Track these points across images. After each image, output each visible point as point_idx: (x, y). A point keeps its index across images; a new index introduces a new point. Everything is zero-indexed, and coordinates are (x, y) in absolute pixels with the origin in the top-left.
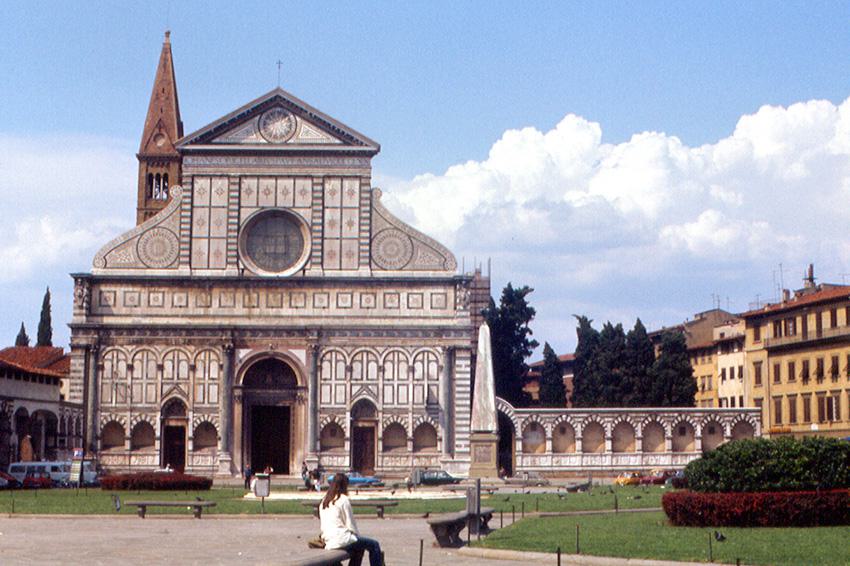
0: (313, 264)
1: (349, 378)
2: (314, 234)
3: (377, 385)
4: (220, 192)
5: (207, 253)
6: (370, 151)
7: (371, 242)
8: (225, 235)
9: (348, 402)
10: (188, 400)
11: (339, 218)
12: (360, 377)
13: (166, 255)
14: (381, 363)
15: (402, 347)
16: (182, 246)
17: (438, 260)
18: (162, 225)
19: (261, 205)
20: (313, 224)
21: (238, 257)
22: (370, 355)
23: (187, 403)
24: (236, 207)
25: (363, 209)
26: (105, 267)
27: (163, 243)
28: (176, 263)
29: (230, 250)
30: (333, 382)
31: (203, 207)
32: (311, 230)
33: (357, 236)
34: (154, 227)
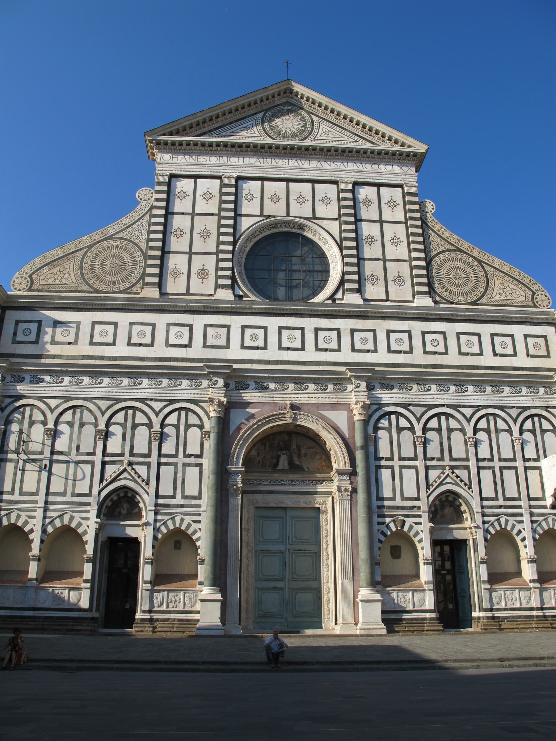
1: (420, 455)
2: (345, 252)
3: (467, 468)
4: (207, 196)
5: (186, 272)
6: (415, 155)
8: (214, 251)
9: (423, 494)
10: (148, 494)
11: (379, 234)
12: (438, 455)
13: (125, 273)
14: (470, 432)
15: (501, 408)
16: (150, 262)
17: (523, 294)
18: (122, 235)
19: (265, 213)
21: (233, 278)
22: (450, 418)
23: (145, 496)
24: (232, 214)
26: (30, 290)
27: (121, 258)
28: (139, 285)
29: (222, 269)
30: (396, 463)
31: (183, 214)
33: (407, 258)
34: (110, 238)
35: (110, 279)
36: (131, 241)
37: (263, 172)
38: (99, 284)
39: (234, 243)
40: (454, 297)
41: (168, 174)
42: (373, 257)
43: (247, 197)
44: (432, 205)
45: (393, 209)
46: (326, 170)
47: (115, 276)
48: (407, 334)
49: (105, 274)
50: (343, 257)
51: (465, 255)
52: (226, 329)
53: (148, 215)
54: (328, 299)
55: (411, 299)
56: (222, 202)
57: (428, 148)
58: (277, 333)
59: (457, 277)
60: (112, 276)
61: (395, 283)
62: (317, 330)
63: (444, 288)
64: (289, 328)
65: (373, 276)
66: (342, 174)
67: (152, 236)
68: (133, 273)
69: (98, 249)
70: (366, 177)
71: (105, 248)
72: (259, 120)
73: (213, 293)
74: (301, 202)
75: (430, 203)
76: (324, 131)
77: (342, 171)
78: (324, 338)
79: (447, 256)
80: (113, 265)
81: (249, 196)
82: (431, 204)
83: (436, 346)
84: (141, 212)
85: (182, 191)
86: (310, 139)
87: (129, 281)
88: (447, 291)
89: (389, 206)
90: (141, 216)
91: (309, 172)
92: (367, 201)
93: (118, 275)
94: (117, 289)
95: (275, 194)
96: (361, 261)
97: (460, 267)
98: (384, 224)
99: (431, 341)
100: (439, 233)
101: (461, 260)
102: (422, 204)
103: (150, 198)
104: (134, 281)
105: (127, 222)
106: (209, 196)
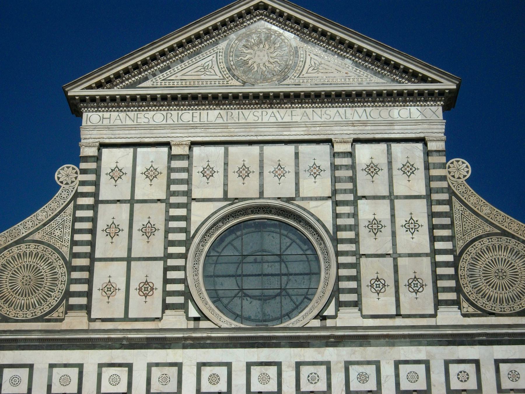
0: (340, 305)
2: (341, 247)
5: (123, 287)
6: (442, 93)
7: (457, 258)
8: (160, 253)
11: (389, 216)
13: (41, 293)
16: (75, 275)
18: (37, 236)
19: (230, 195)
20: (337, 228)
25: (435, 197)
27: (37, 270)
28: (61, 309)
31: (118, 201)
32: (336, 241)
33: (428, 251)
35: (23, 301)
36: (49, 245)
37: (227, 134)
38: (8, 309)
39: (187, 243)
40: (494, 305)
41: (98, 144)
42: (379, 252)
43: (205, 172)
44: (467, 167)
45: (409, 176)
46: (315, 124)
47: (29, 296)
48: (423, 366)
49: (16, 294)
50: (338, 254)
51: (513, 240)
52: (177, 368)
53: (71, 205)
54: (315, 318)
55: (432, 312)
56: (170, 182)
57: (460, 83)
58: (245, 372)
59: (500, 274)
60: (25, 296)
61: (410, 289)
62: (298, 365)
63: (479, 293)
64: (261, 364)
65: (379, 280)
66: (337, 130)
67: (77, 237)
68: (53, 291)
69: (5, 259)
70: (371, 132)
71: (14, 257)
72: (221, 54)
73: (160, 316)
74: (279, 175)
75: (463, 163)
76: (313, 64)
77: (337, 124)
78: (309, 376)
79: (487, 243)
80: (26, 280)
81: (208, 170)
82: (465, 165)
83: (465, 381)
84: (62, 201)
85: (117, 167)
86: (293, 77)
87: (48, 303)
88: (484, 297)
89: (404, 173)
90: (62, 207)
91: (292, 129)
92: (372, 167)
93: (32, 295)
94: (33, 316)
95: (244, 165)
96: (363, 260)
97: (505, 260)
98: (396, 202)
99: (458, 375)
100: (476, 209)
101: (506, 248)
102: (451, 165)
103: (74, 180)
104: (55, 304)
105: (44, 218)
106: (154, 173)
